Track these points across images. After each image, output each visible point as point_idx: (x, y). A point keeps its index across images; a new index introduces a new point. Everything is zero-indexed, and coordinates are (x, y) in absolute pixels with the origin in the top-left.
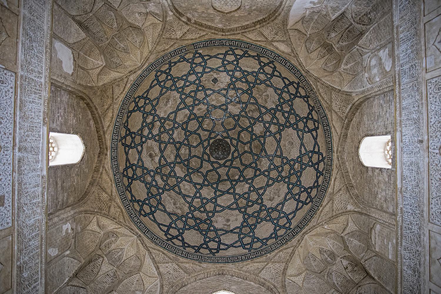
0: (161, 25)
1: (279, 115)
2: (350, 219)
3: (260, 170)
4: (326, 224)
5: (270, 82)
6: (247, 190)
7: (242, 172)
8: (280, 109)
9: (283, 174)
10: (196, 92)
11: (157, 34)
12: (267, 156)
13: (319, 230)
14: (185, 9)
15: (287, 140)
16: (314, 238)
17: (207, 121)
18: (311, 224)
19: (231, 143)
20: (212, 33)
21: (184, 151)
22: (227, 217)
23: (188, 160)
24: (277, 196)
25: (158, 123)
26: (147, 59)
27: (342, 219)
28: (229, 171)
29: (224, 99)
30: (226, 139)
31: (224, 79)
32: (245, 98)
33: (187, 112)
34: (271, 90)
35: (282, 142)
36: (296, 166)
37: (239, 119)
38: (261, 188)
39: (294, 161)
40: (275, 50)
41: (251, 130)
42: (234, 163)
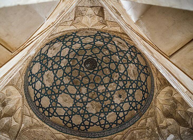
0: (158, 123)
1: (81, 105)
2: (18, 124)
3: (65, 76)
4: (21, 109)
5: (98, 116)
6: (61, 65)
7: (71, 66)
8: (84, 108)
9: (55, 88)
10: (125, 85)
11: (158, 117)
12: (68, 84)
13: (20, 104)
14: (153, 135)
15: (68, 100)
16: (18, 99)
17: (108, 73)
18: (25, 101)
19: (89, 72)
20: (135, 127)
21: (107, 52)
22: (56, 49)
23: (101, 50)
24: (47, 79)
25: (130, 60)
26: (155, 102)
27: (20, 119)
28: (77, 61)
29: (110, 89)
30: (92, 71)
31: (117, 100)
32: (101, 98)
33: (121, 72)
34: (94, 112)
35: (69, 96)
36: (54, 97)
37: (96, 85)
38: (56, 72)
39: (57, 98)
40: (107, 137)
41: (86, 86)
42: (79, 65)
